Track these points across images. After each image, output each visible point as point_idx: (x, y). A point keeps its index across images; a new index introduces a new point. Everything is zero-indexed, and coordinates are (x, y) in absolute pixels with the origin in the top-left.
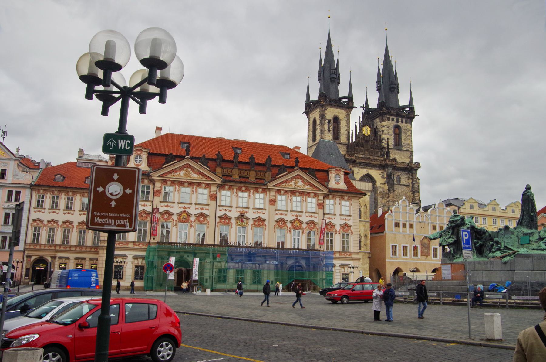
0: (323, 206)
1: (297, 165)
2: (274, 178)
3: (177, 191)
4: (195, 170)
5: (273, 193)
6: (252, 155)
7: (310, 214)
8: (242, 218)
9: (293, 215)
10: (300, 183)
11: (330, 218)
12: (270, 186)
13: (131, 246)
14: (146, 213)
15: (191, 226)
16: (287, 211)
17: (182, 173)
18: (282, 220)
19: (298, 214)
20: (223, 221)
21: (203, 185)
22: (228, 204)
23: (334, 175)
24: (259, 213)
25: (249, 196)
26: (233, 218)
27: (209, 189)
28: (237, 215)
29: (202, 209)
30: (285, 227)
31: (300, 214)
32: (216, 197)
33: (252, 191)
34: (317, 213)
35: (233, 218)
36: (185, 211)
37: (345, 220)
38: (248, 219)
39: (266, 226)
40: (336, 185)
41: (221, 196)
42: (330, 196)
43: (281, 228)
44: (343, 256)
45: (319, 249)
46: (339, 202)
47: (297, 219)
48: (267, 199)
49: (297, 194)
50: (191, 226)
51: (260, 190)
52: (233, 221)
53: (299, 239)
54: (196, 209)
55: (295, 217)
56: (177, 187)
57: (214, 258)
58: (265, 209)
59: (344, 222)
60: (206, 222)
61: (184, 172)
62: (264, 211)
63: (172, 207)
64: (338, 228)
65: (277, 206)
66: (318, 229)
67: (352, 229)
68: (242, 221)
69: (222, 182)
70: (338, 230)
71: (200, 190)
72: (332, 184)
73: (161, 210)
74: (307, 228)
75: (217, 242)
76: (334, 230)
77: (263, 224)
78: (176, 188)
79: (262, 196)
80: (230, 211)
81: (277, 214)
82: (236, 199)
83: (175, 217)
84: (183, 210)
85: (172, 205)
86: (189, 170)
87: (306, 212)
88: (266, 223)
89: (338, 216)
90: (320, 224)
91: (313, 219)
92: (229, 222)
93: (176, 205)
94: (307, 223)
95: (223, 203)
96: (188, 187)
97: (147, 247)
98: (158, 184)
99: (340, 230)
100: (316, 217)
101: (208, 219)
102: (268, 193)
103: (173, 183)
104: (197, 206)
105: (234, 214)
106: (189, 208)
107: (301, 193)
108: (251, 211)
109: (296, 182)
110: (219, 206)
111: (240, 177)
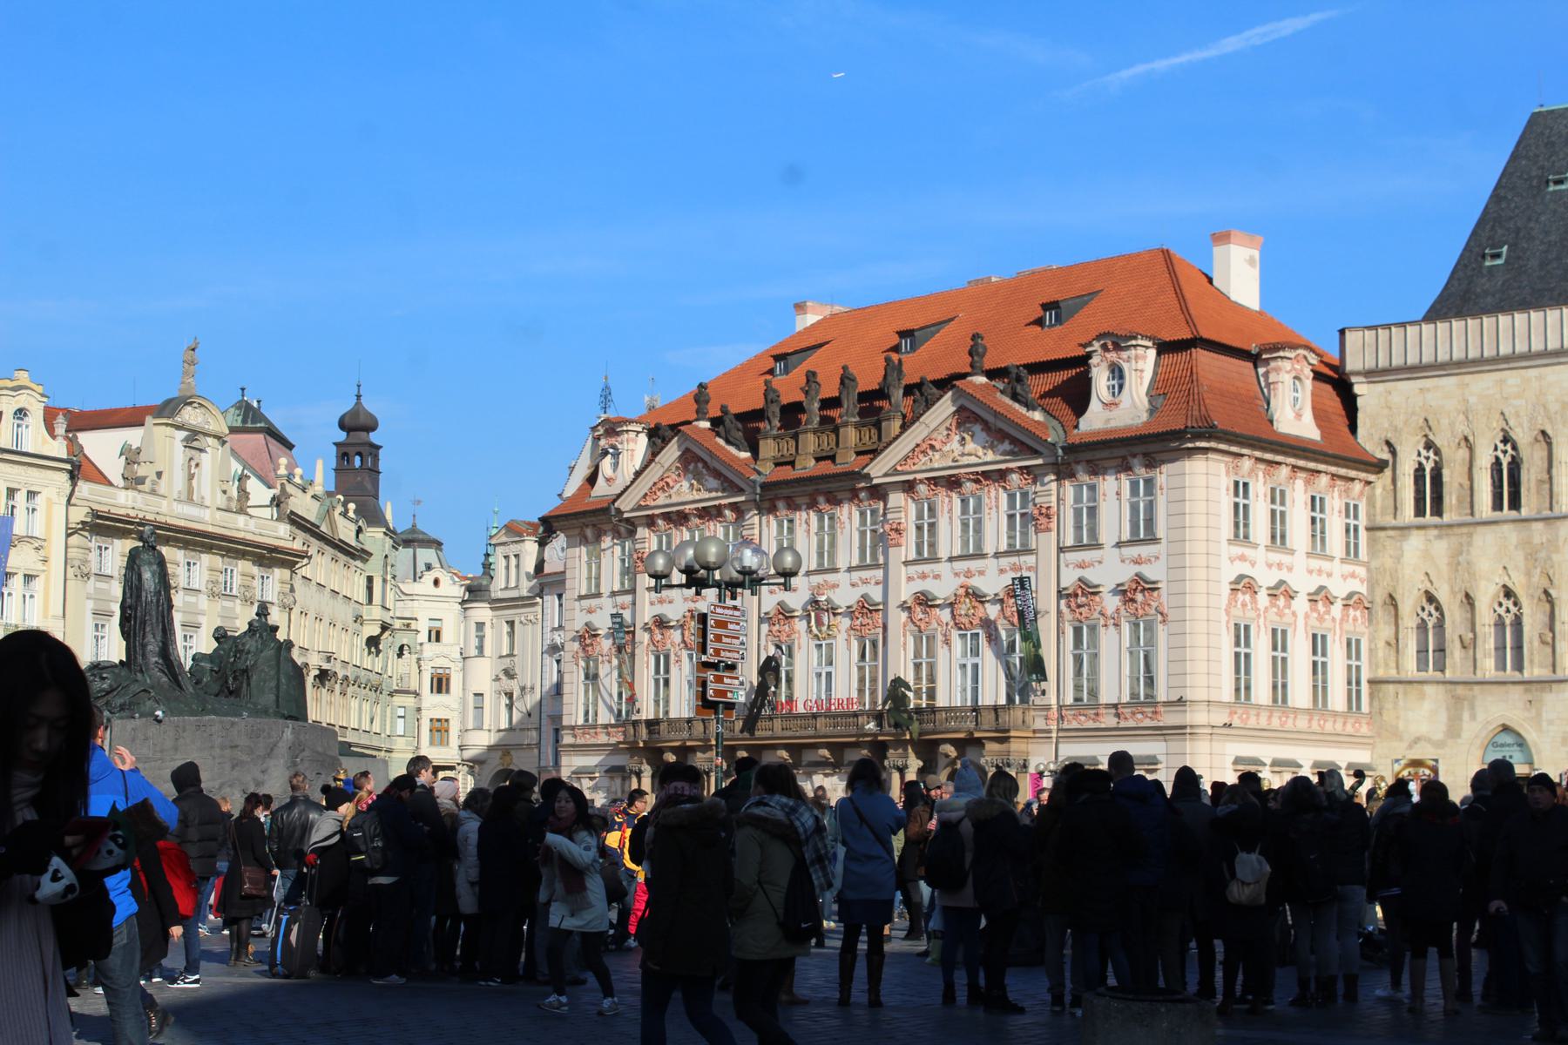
1: (975, 369)
6: (845, 368)
9: (956, 574)
11: (1082, 566)
20: (777, 627)
24: (865, 582)
37: (1137, 562)
38: (833, 610)
40: (1107, 414)
44: (1131, 723)
49: (969, 486)
55: (962, 580)
59: (1137, 569)
67: (1164, 599)
68: (819, 623)
70: (1110, 611)
76: (1096, 615)
89: (1109, 554)
108: (841, 578)
111: (818, 459)
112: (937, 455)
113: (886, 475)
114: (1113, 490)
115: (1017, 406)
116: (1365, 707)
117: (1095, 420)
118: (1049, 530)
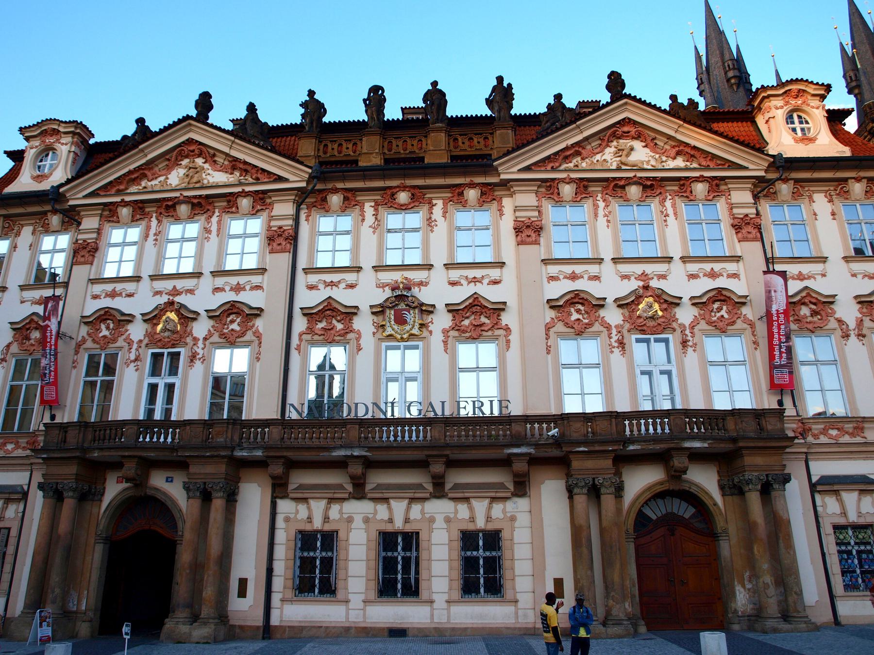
0: (759, 228)
3: (151, 237)
4: (220, 159)
5: (527, 199)
6: (435, 84)
7: (707, 267)
10: (641, 154)
11: (801, 277)
12: (510, 170)
14: (38, 327)
15: (193, 358)
16: (600, 261)
17: (175, 177)
18: (577, 299)
19: (649, 268)
20: (321, 325)
21: (245, 203)
22: (343, 260)
23: (780, 115)
24: (475, 280)
25: (430, 222)
26: (365, 308)
27: (265, 214)
28: (381, 296)
29: (238, 289)
30: (597, 327)
31: (661, 268)
32: (294, 239)
34: (737, 259)
35: (365, 308)
36: (172, 303)
39: (507, 329)
41: (315, 234)
42: (785, 189)
43: (579, 332)
45: (775, 406)
46: (829, 207)
47: (646, 288)
48: (507, 223)
49: (634, 191)
50: (193, 358)
51: (472, 194)
52: (364, 324)
54: (217, 290)
56: (154, 222)
57: (279, 489)
58: (502, 265)
60: (249, 336)
61: (182, 171)
62: (494, 273)
63: (130, 295)
64: (847, 311)
65: (549, 249)
66: (752, 325)
68: (401, 320)
69: (311, 178)
71: (236, 226)
73: (92, 307)
74: (703, 325)
77: (496, 325)
78: (148, 228)
79: (483, 217)
80: (352, 286)
81: (552, 278)
82: (375, 237)
83: (137, 331)
84: (164, 299)
85: (130, 287)
86: (199, 161)
87: (685, 259)
88: (506, 319)
90: (758, 296)
91: (722, 282)
92: (348, 330)
93: (145, 282)
94: (696, 302)
95: (323, 261)
96: (191, 218)
97: (28, 452)
98: (90, 223)
100: (735, 276)
101: (259, 323)
102: (507, 203)
103: (140, 211)
104: (220, 281)
105: (367, 294)
106: (191, 291)
107: (652, 186)
108: (439, 277)
109: (619, 151)
110: (306, 271)
112: (584, 165)
118: (754, 239)
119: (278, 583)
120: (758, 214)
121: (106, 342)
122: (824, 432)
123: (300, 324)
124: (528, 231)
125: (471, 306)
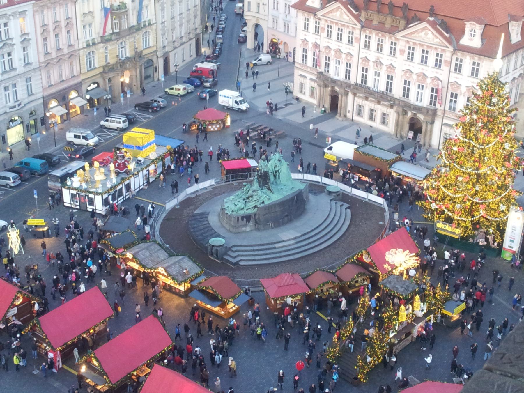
2: (406, 28)
8: (378, 63)
10: (430, 35)
11: (456, 78)
12: (399, 35)
13: (309, 70)
28: (374, 60)
33: (387, 38)
38: (381, 64)
52: (371, 64)
53: (422, 93)
55: (421, 71)
64: (463, 89)
68: (377, 66)
70: (463, 92)
72: (465, 41)
75: (359, 82)
88: (396, 71)
92: (368, 65)
99: (465, 92)
113: (402, 36)
114: (468, 62)
115: (443, 31)
116: (517, 101)
117: (465, 41)
119: (354, 112)
120: (452, 59)
121: (328, 54)
122: (449, 114)
123: (360, 61)
124: (402, 52)
125: (390, 67)
